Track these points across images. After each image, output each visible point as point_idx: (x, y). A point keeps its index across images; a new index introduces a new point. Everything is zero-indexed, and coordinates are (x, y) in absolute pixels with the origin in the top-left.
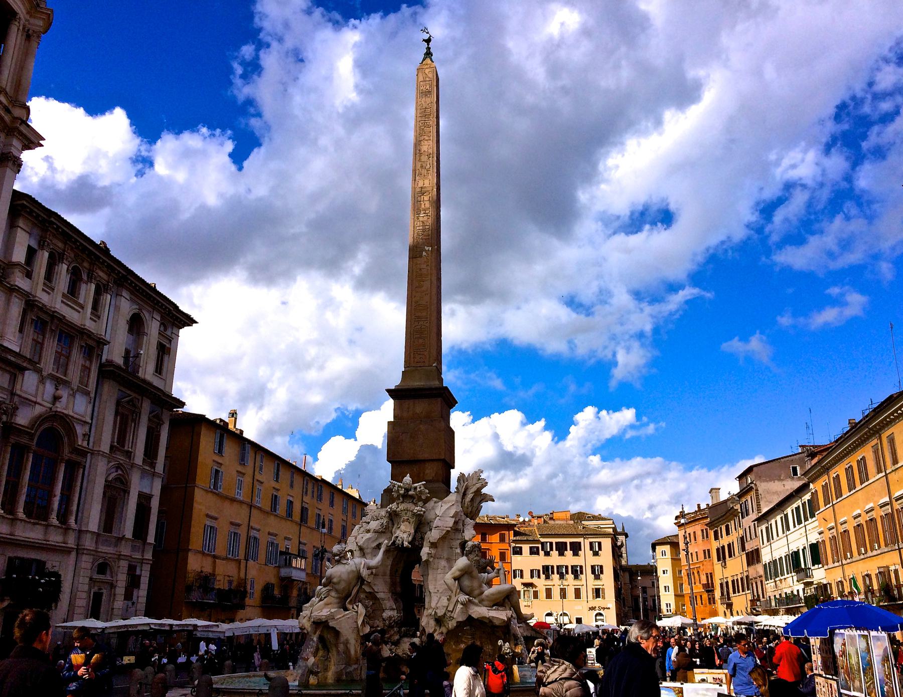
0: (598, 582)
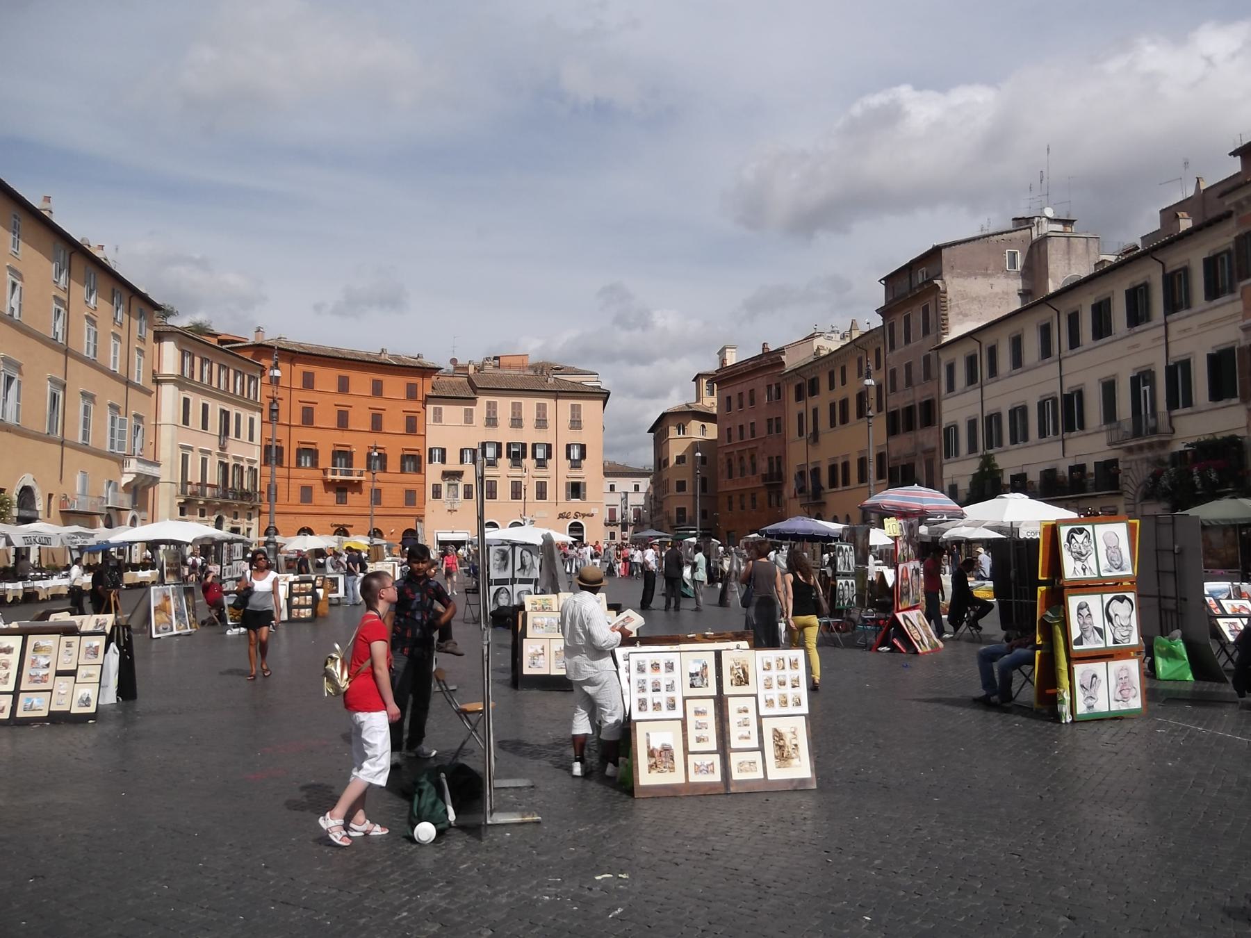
0: (576, 473)
